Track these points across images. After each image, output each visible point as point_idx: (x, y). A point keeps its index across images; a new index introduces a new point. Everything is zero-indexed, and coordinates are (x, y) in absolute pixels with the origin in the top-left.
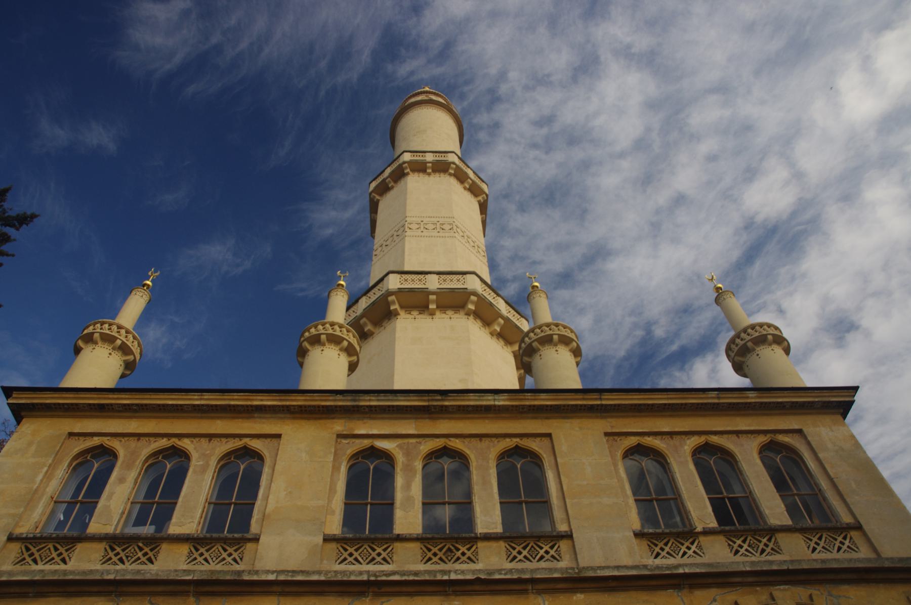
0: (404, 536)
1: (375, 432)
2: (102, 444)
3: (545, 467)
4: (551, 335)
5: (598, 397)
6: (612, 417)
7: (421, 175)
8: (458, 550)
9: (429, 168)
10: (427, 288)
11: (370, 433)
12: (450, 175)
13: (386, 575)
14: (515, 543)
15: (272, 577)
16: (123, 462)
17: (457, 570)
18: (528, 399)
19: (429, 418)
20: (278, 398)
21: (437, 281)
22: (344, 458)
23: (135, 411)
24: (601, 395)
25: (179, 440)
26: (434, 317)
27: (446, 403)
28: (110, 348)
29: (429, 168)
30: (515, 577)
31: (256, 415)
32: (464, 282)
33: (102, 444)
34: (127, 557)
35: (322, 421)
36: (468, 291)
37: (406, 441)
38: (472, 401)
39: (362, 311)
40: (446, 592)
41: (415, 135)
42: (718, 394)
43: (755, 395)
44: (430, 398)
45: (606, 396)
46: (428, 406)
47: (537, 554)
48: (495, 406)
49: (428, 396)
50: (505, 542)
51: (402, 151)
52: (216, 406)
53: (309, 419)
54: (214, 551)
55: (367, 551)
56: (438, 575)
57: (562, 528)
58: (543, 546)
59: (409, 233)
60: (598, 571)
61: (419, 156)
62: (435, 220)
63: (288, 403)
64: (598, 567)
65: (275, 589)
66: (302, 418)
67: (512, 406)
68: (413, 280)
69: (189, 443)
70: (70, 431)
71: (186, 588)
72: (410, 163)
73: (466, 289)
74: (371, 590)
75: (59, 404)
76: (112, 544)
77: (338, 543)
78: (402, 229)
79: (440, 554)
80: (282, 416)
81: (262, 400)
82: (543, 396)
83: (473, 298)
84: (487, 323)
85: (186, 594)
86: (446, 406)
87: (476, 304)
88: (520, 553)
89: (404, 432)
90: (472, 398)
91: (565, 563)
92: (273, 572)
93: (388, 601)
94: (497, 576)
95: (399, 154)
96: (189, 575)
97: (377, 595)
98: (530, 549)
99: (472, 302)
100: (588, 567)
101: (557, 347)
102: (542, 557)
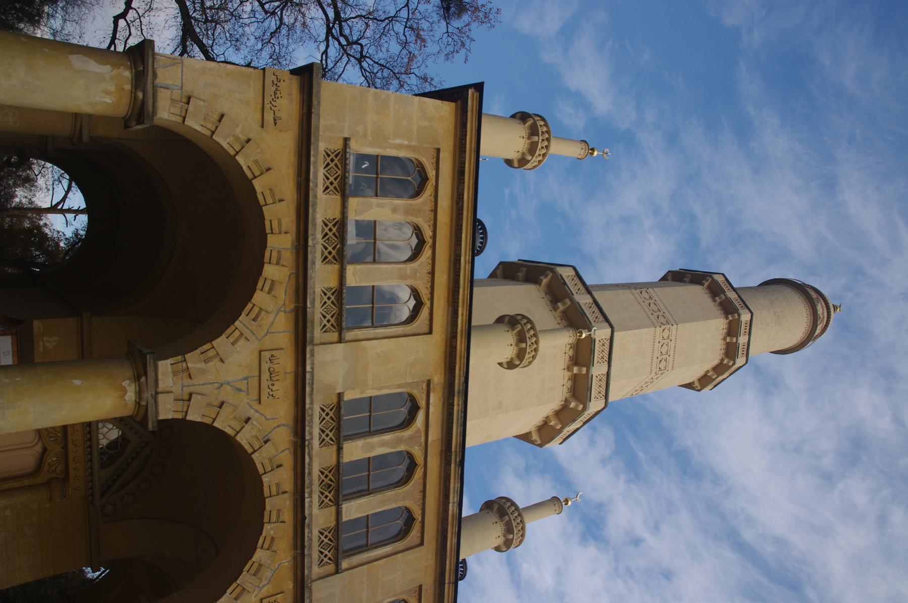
0: (341, 453)
1: (431, 409)
2: (429, 179)
3: (395, 544)
4: (513, 533)
5: (451, 581)
6: (435, 589)
7: (725, 331)
8: (330, 492)
9: (731, 340)
10: (593, 366)
11: (431, 406)
12: (722, 360)
13: (309, 452)
14: (334, 532)
15: (308, 368)
16: (411, 205)
17: (312, 502)
18: (453, 528)
19: (442, 450)
20: (464, 328)
21: (600, 373)
22: (410, 389)
23: (458, 203)
24: (453, 583)
25: (430, 247)
26: (566, 370)
27: (453, 466)
28: (524, 150)
29: (731, 340)
30: (306, 544)
31: (450, 308)
32: (597, 398)
33: (429, 179)
34: (328, 239)
35: (443, 365)
36: (588, 403)
37: (423, 435)
38: (453, 485)
39: (577, 301)
40: (297, 493)
41: (775, 314)
44: (458, 453)
46: (451, 451)
47: (325, 549)
48: (449, 503)
49: (460, 452)
50: (335, 526)
51: (753, 312)
52: (459, 276)
53: (445, 352)
54: (332, 308)
55: (330, 426)
56: (309, 489)
57: (345, 564)
58: (331, 553)
59: (659, 330)
60: (308, 600)
61: (746, 329)
62: (671, 353)
63: (459, 337)
64: (311, 600)
65: (300, 369)
66: (446, 346)
67: (448, 516)
68: (603, 351)
69: (427, 256)
70: (441, 149)
71: (301, 300)
72: (739, 321)
73: (590, 401)
74: (299, 440)
75: (466, 135)
76: (339, 223)
77: (337, 403)
78: (664, 322)
79: (326, 480)
80: (449, 331)
81: (462, 315)
82: (455, 540)
83: (581, 407)
84: (558, 414)
85: (297, 301)
86: (450, 465)
87: (575, 410)
88: (326, 537)
89: (430, 433)
90: (456, 485)
91: (316, 570)
92: (312, 368)
93: (290, 453)
94: (306, 531)
95: (750, 307)
96: (311, 304)
97: (295, 445)
98: (329, 544)
99: (577, 406)
100: (311, 592)
101: (502, 537)
102: (322, 553)
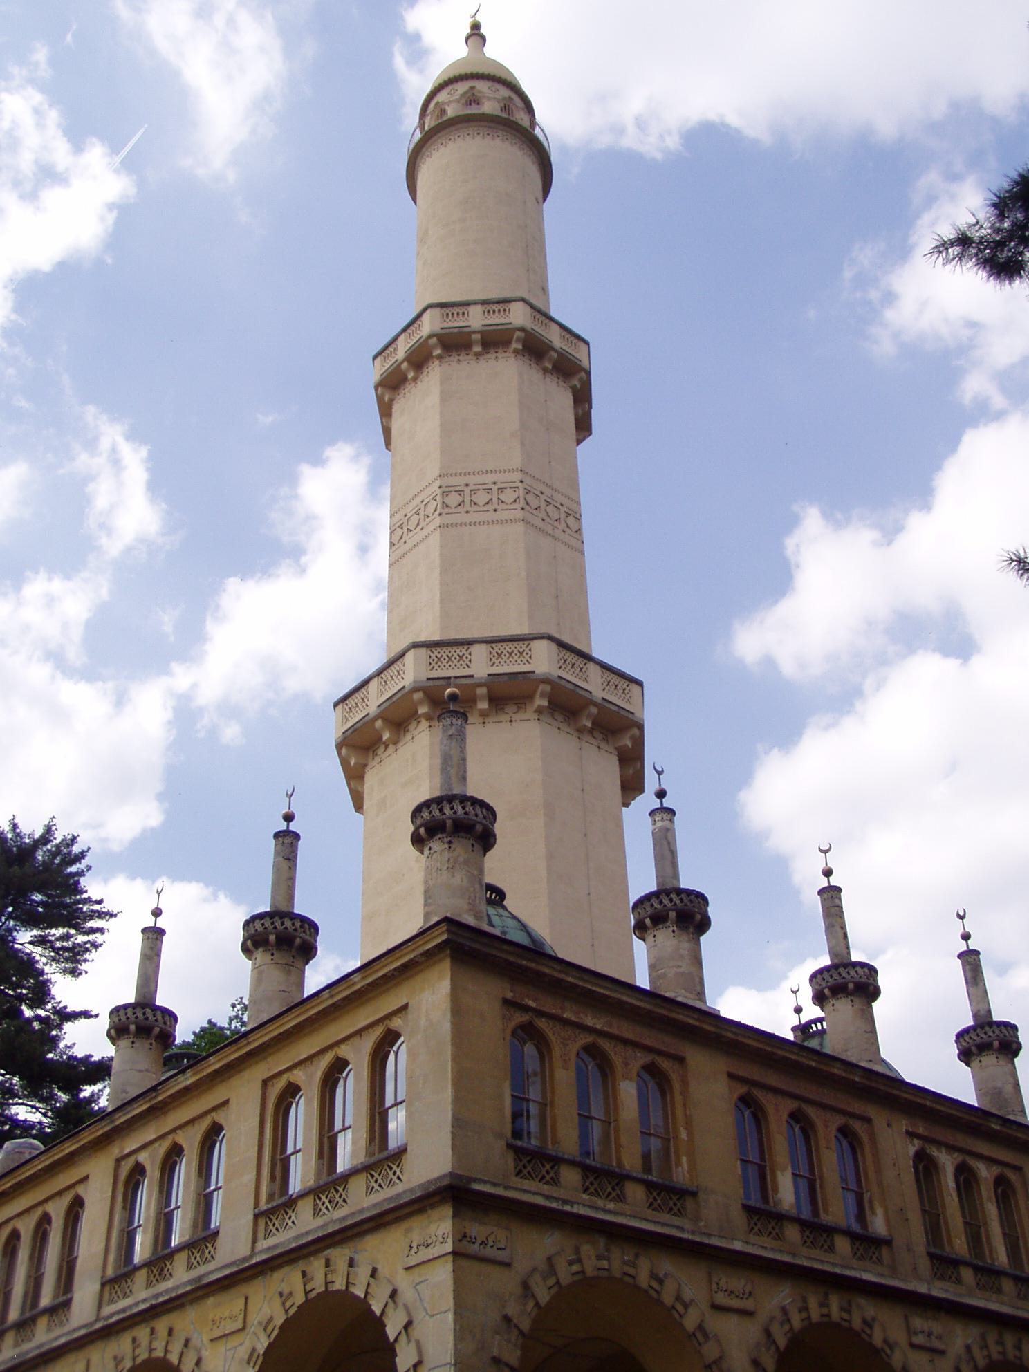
10: (368, 714)
27: (160, 1098)
42: (330, 992)
43: (360, 977)
45: (252, 1037)
94: (161, 1299)
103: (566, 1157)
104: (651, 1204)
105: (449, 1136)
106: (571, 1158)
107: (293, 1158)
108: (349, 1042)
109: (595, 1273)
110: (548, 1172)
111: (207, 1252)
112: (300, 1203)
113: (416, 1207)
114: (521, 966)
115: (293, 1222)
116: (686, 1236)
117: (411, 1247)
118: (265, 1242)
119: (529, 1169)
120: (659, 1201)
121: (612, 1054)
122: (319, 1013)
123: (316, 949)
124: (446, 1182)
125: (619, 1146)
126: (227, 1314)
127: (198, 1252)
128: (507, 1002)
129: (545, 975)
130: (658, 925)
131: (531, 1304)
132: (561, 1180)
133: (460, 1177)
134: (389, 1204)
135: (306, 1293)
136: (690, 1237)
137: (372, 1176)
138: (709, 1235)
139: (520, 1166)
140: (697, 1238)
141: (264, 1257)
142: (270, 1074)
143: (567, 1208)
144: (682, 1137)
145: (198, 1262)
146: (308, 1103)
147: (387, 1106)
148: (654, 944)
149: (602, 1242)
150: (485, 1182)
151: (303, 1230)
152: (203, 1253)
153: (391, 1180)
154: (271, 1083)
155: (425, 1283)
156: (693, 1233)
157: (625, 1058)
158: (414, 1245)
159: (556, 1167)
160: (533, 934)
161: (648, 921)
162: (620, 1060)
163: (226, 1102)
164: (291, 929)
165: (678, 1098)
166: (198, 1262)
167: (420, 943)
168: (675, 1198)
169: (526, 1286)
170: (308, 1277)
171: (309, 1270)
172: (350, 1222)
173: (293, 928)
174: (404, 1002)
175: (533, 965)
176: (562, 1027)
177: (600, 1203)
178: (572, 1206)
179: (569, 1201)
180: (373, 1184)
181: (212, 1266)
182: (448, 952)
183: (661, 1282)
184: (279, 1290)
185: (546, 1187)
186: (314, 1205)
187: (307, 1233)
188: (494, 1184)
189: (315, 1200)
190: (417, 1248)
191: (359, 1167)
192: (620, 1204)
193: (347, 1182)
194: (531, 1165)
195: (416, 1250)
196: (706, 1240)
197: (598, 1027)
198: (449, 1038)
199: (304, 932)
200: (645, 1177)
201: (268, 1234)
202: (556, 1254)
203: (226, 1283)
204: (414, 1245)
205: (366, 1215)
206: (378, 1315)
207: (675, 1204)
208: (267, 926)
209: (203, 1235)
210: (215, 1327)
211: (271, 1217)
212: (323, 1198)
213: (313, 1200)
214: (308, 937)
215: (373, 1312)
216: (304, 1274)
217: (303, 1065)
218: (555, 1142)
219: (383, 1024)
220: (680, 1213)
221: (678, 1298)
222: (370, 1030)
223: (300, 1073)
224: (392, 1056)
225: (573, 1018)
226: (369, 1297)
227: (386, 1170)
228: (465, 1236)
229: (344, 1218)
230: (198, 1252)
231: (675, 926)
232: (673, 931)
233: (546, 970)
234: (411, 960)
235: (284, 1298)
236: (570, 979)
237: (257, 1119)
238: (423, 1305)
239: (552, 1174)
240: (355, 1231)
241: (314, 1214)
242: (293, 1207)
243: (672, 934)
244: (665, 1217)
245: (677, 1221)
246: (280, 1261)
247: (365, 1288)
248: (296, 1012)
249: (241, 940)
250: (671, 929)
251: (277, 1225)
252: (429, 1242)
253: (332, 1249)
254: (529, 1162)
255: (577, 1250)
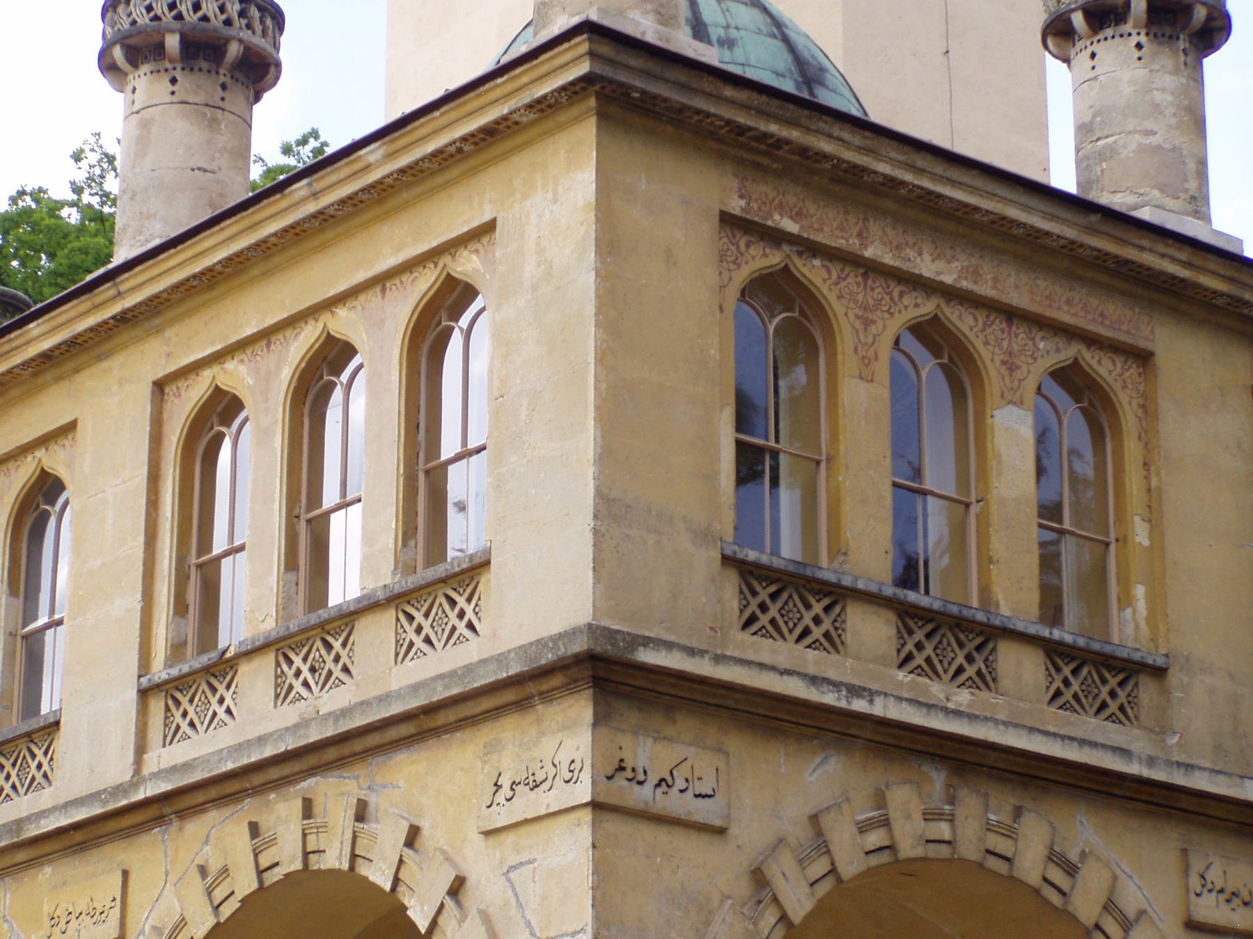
6: (171, 322)
42: (309, 185)
43: (381, 152)
45: (127, 281)
103: (861, 585)
104: (1058, 693)
105: (589, 538)
106: (873, 588)
107: (226, 563)
108: (355, 303)
109: (919, 852)
110: (817, 621)
111: (34, 765)
112: (244, 669)
113: (509, 696)
114: (766, 136)
115: (229, 711)
116: (1133, 769)
117: (498, 786)
118: (164, 751)
119: (773, 612)
120: (1075, 686)
121: (978, 343)
122: (285, 230)
123: (278, 65)
124: (579, 646)
125: (986, 561)
126: (82, 906)
127: (14, 765)
128: (727, 220)
129: (826, 157)
130: (1101, 28)
131: (770, 917)
132: (848, 637)
133: (611, 634)
134: (447, 687)
135: (260, 873)
136: (1146, 773)
137: (411, 618)
138: (1189, 767)
139: (753, 607)
140: (1159, 775)
141: (164, 787)
142: (172, 368)
143: (859, 705)
144: (1138, 539)
145: (14, 787)
146: (263, 436)
147: (445, 456)
148: (1091, 74)
149: (938, 778)
150: (669, 646)
151: (252, 734)
152: (24, 767)
153: (454, 629)
154: (174, 388)
155: (531, 866)
156: (1151, 762)
157: (1011, 354)
158: (505, 782)
159: (837, 609)
160: (800, 43)
161: (1078, 19)
162: (997, 359)
163: (71, 427)
164: (217, 22)
165: (1132, 448)
166: (14, 787)
167: (525, 79)
168: (1113, 682)
169: (759, 878)
170: (266, 834)
171: (267, 822)
172: (358, 721)
173: (224, 17)
174: (487, 217)
175: (794, 134)
176: (860, 279)
177: (936, 690)
178: (871, 702)
179: (864, 689)
180: (411, 635)
181: (45, 798)
182: (592, 102)
183: (1071, 870)
184: (199, 861)
185: (811, 654)
186: (277, 677)
187: (261, 740)
188: (691, 652)
189: (278, 664)
190: (512, 789)
191: (381, 595)
192: (984, 695)
193: (353, 628)
194: (779, 604)
195: (510, 794)
196: (1179, 779)
197: (948, 279)
198: (590, 309)
199: (249, 26)
200: (1045, 632)
201: (172, 735)
202: (828, 809)
203: (78, 837)
204: (505, 782)
205: (396, 708)
206: (423, 931)
207: (1113, 694)
208: (159, 12)
209: (25, 728)
210: (57, 930)
211: (178, 695)
212: (298, 661)
213: (273, 665)
214: (257, 40)
215: (412, 925)
216: (254, 829)
217: (249, 351)
218: (837, 550)
219: (436, 265)
220: (1124, 715)
221: (1110, 906)
222: (406, 277)
223: (243, 369)
224: (455, 342)
225: (888, 259)
226: (401, 888)
227: (441, 605)
228: (622, 769)
229: (344, 713)
230: (14, 765)
231: (1143, 32)
232: (1139, 46)
233: (827, 147)
234: (505, 118)
235: (209, 880)
236: (884, 168)
237: (144, 471)
238: (524, 916)
239: (827, 625)
240: (374, 739)
241: (277, 696)
242: (228, 678)
243: (1137, 54)
244: (1089, 725)
245: (1115, 734)
246: (200, 797)
247: (394, 870)
248: (231, 226)
249: (98, 44)
250: (1134, 40)
251: (191, 714)
252: (539, 778)
253: (318, 778)
254: (774, 596)
255: (880, 800)
